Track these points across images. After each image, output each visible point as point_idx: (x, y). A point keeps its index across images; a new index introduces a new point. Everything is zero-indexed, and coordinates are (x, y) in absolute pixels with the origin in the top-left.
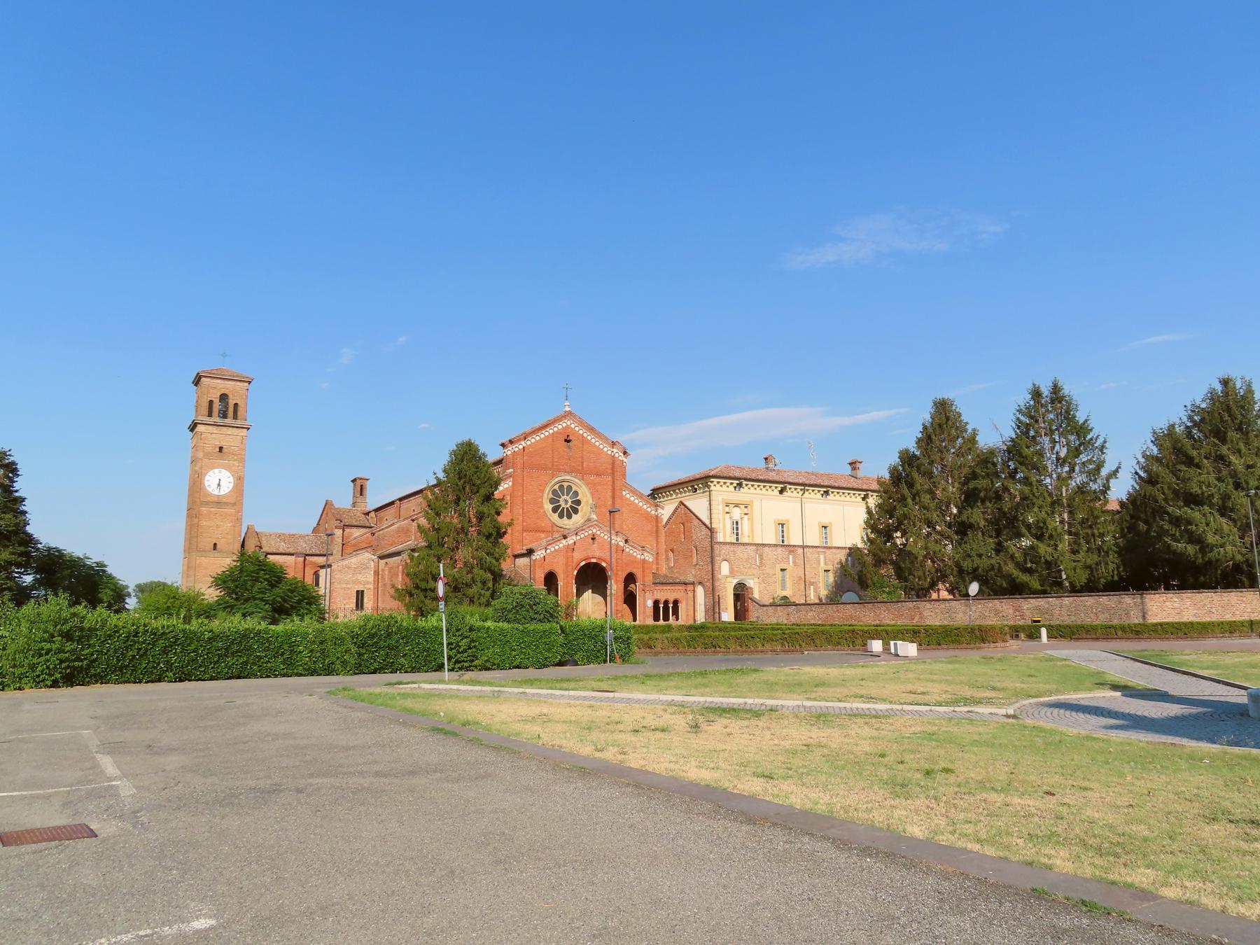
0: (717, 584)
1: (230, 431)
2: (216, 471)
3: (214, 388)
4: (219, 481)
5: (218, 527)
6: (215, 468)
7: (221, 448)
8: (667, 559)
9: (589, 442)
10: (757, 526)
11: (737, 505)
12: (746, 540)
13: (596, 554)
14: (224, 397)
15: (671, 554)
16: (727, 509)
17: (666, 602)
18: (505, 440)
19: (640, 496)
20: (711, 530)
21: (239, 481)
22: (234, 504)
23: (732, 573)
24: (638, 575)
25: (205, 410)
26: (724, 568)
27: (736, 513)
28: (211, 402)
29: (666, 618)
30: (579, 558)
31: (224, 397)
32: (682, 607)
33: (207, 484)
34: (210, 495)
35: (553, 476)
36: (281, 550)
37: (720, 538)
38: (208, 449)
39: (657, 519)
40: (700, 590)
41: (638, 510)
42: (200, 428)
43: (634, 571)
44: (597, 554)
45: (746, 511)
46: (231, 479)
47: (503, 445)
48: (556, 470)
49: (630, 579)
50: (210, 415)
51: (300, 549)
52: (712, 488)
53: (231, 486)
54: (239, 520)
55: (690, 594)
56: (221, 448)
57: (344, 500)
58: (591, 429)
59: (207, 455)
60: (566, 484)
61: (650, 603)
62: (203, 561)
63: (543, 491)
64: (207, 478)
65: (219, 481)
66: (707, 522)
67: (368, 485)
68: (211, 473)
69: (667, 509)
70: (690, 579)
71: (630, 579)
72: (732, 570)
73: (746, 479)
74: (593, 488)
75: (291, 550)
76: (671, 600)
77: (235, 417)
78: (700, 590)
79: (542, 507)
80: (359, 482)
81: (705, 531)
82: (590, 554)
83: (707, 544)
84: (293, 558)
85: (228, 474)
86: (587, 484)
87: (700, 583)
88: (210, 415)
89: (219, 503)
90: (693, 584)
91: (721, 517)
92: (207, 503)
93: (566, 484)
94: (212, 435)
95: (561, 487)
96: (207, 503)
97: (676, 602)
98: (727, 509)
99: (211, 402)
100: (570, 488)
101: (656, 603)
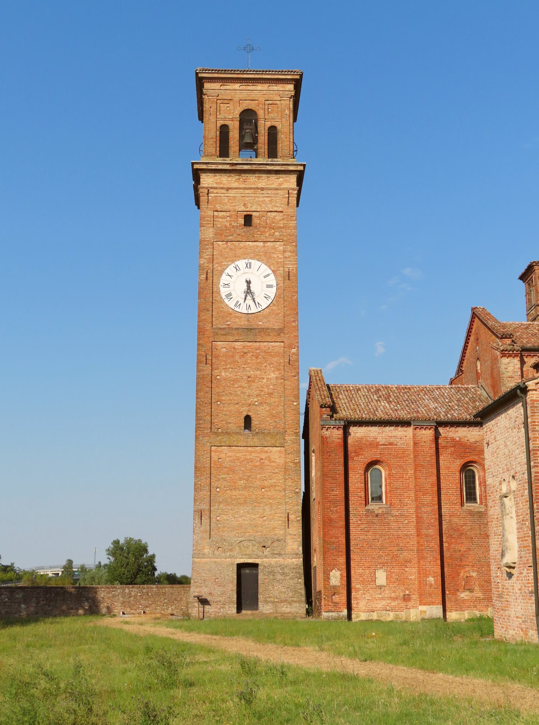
1: (263, 181)
2: (242, 263)
3: (228, 102)
4: (248, 283)
5: (250, 380)
7: (248, 220)
14: (248, 118)
21: (288, 281)
22: (280, 331)
25: (213, 147)
28: (224, 130)
31: (248, 118)
33: (224, 292)
34: (231, 313)
36: (380, 415)
38: (223, 221)
42: (206, 180)
46: (272, 280)
50: (224, 152)
53: (272, 292)
54: (292, 364)
56: (248, 220)
59: (221, 235)
64: (224, 279)
65: (248, 283)
68: (230, 270)
75: (403, 415)
77: (273, 153)
84: (409, 431)
85: (265, 269)
88: (224, 152)
89: (251, 330)
92: (228, 331)
94: (229, 194)
99: (224, 130)
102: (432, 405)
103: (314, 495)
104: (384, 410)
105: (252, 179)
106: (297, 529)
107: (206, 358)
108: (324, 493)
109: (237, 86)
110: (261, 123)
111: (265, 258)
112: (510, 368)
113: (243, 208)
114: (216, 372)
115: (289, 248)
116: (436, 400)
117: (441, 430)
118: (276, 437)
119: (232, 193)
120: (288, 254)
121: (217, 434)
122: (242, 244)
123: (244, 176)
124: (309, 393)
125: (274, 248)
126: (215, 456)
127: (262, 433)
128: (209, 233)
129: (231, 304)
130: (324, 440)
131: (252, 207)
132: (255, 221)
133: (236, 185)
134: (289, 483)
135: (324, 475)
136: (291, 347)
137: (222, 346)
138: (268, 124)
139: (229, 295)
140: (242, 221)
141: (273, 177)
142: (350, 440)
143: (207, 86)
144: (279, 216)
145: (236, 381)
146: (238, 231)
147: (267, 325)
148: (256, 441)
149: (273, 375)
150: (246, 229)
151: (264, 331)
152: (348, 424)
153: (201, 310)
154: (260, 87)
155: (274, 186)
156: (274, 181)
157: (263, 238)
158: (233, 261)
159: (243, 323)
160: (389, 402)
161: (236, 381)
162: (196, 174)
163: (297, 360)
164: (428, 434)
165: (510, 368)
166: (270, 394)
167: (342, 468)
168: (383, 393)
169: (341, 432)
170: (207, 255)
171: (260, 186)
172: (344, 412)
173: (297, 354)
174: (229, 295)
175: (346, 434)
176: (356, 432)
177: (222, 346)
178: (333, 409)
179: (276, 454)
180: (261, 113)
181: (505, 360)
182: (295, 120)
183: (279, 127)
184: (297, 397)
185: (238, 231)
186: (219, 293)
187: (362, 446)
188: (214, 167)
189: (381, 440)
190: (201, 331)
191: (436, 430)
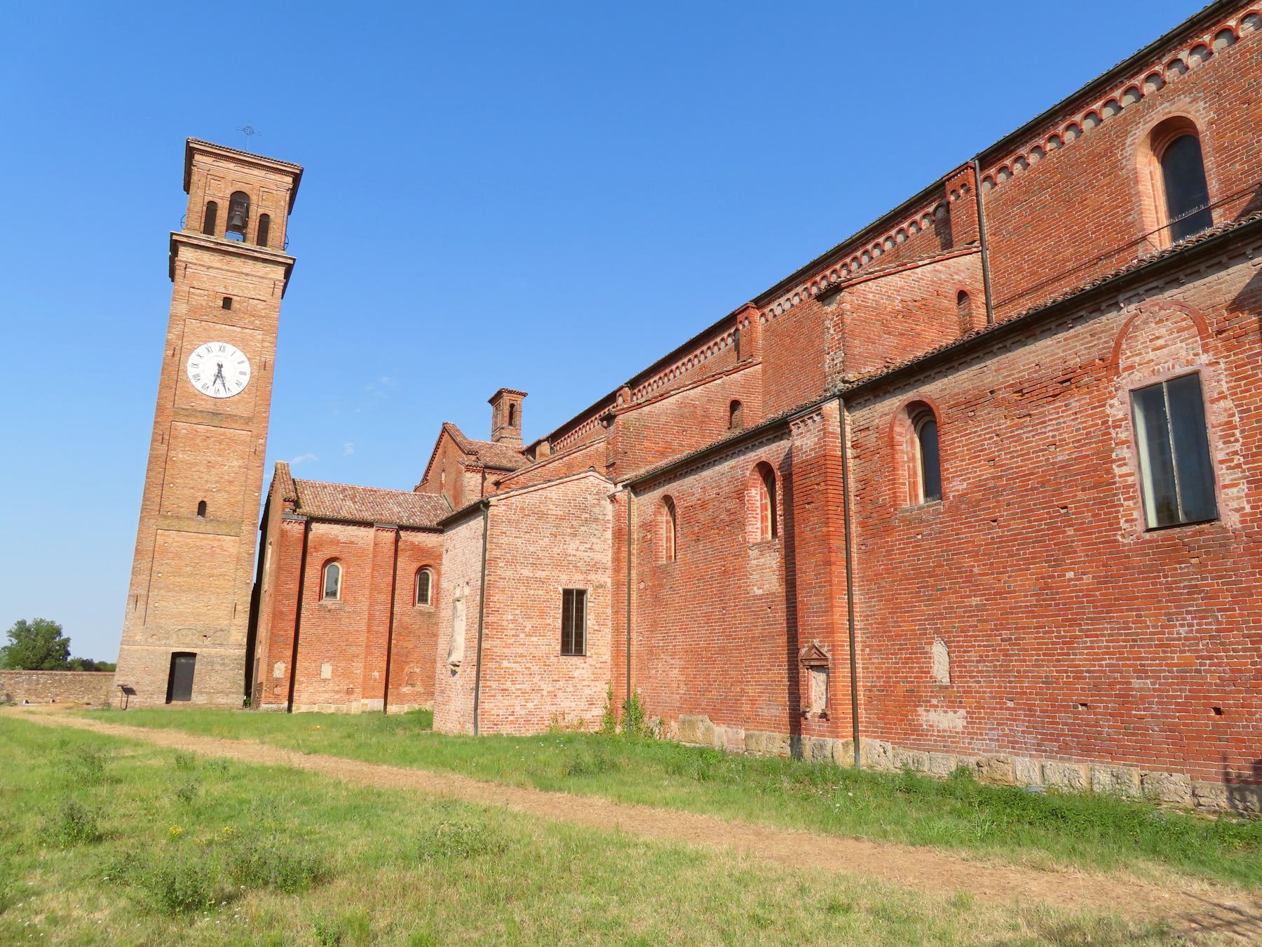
2: (215, 346)
3: (219, 180)
4: (219, 367)
6: (211, 339)
7: (227, 303)
14: (239, 200)
22: (248, 420)
25: (198, 222)
28: (212, 208)
31: (239, 200)
33: (191, 371)
34: (198, 395)
36: (344, 514)
38: (199, 299)
42: (185, 254)
46: (246, 367)
50: (209, 228)
51: (386, 515)
53: (245, 380)
56: (227, 303)
57: (477, 427)
59: (194, 312)
62: (173, 539)
64: (193, 358)
65: (219, 367)
67: (524, 405)
68: (201, 350)
75: (367, 516)
77: (262, 240)
80: (506, 400)
85: (240, 355)
88: (209, 228)
89: (217, 414)
92: (191, 413)
94: (208, 272)
99: (212, 208)
102: (396, 509)
103: (266, 586)
104: (348, 509)
105: (237, 262)
106: (243, 620)
107: (162, 437)
108: (277, 587)
109: (231, 165)
110: (253, 208)
111: (242, 344)
112: (472, 483)
114: (172, 453)
115: (268, 338)
116: (400, 505)
117: (402, 533)
118: (231, 526)
119: (212, 273)
120: (266, 344)
121: (166, 517)
122: (218, 326)
123: (228, 258)
124: (272, 486)
125: (252, 335)
127: (215, 520)
128: (182, 309)
129: (198, 385)
130: (283, 534)
131: (232, 291)
132: (235, 305)
133: (218, 265)
134: (240, 573)
135: (279, 568)
136: (258, 437)
137: (182, 427)
138: (261, 211)
139: (197, 377)
140: (221, 303)
141: (260, 265)
142: (311, 536)
143: (197, 157)
144: (261, 305)
145: (195, 464)
146: (215, 312)
147: (234, 412)
148: (209, 528)
149: (235, 463)
150: (224, 311)
151: (230, 417)
152: (310, 520)
153: (163, 386)
154: (256, 172)
155: (260, 274)
156: (260, 269)
157: (241, 324)
158: (205, 342)
159: (209, 406)
160: (355, 503)
161: (195, 464)
162: (175, 246)
163: (264, 451)
164: (389, 536)
165: (472, 483)
166: (230, 482)
167: (299, 563)
168: (349, 493)
169: (302, 527)
170: (177, 330)
171: (245, 271)
172: (308, 508)
173: (264, 445)
174: (197, 377)
175: (307, 529)
177: (182, 427)
178: (297, 504)
179: (230, 544)
180: (254, 198)
181: (468, 475)
182: (289, 212)
183: (272, 217)
184: (259, 488)
185: (215, 312)
186: (185, 372)
187: (321, 543)
188: (195, 242)
189: (342, 538)
190: (160, 409)
191: (397, 533)
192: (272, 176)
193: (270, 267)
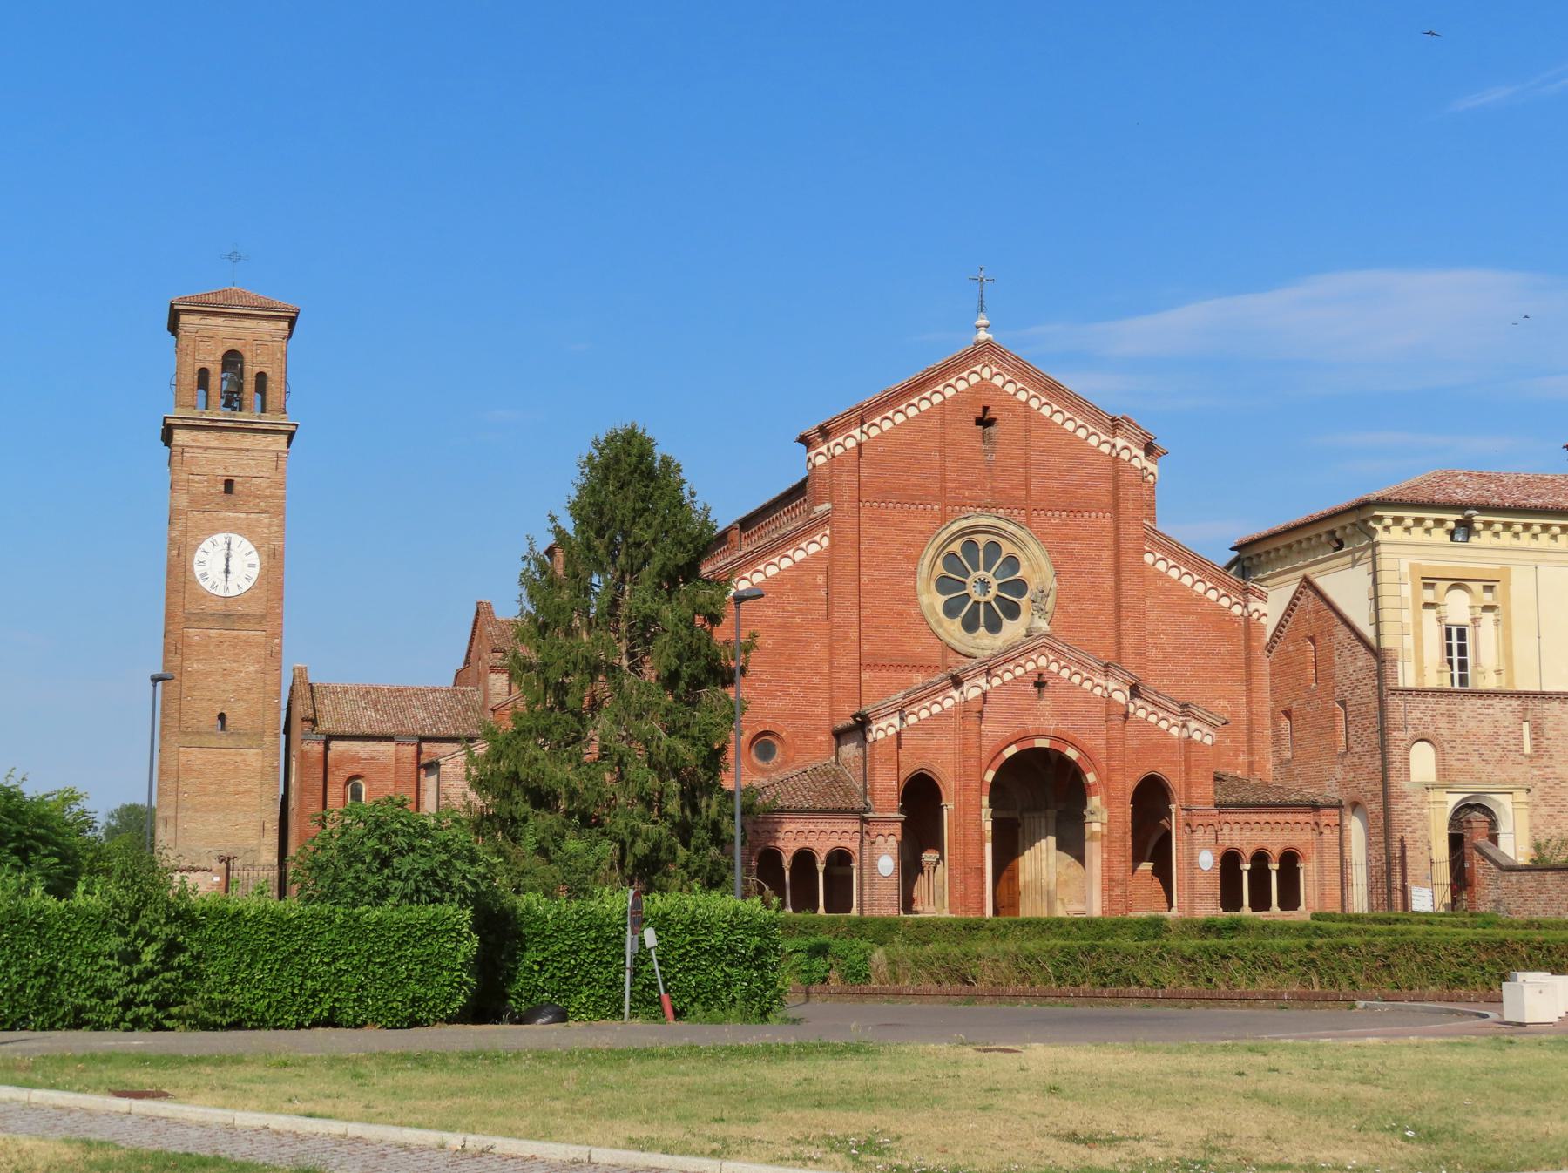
0: (1397, 807)
1: (248, 441)
3: (212, 337)
4: (226, 564)
5: (226, 673)
6: (215, 531)
7: (229, 485)
8: (1277, 739)
9: (1046, 423)
10: (1523, 646)
11: (1458, 584)
12: (1490, 682)
13: (1045, 724)
14: (232, 360)
15: (1285, 723)
16: (1429, 596)
17: (1260, 858)
18: (810, 427)
19: (1198, 564)
20: (1377, 653)
21: (273, 560)
22: (263, 618)
23: (1446, 778)
24: (1175, 781)
26: (1422, 763)
27: (1458, 607)
29: (1261, 902)
30: (1001, 736)
31: (232, 360)
32: (1308, 874)
33: (198, 570)
35: (944, 519)
36: (364, 729)
37: (1406, 676)
38: (200, 487)
39: (1249, 626)
40: (1355, 828)
41: (1190, 604)
42: (180, 437)
43: (1163, 771)
44: (1051, 726)
45: (1488, 598)
46: (255, 558)
47: (804, 440)
48: (949, 502)
49: (1151, 798)
51: (409, 725)
52: (1381, 536)
53: (255, 573)
54: (275, 656)
55: (1330, 837)
56: (229, 485)
58: (1052, 389)
59: (196, 502)
60: (982, 540)
61: (1207, 860)
62: (195, 756)
63: (915, 560)
65: (226, 564)
66: (1369, 633)
69: (1271, 604)
70: (1332, 793)
71: (1151, 798)
72: (1443, 767)
73: (1484, 509)
74: (1057, 545)
75: (388, 728)
76: (1275, 850)
78: (1355, 828)
79: (915, 602)
81: (1364, 659)
82: (1031, 727)
83: (1369, 692)
84: (391, 746)
86: (1041, 539)
87: (1355, 806)
89: (228, 615)
90: (1338, 806)
91: (1407, 617)
92: (200, 618)
93: (982, 540)
94: (210, 455)
95: (970, 547)
96: (200, 618)
97: (1290, 859)
98: (1429, 596)
99: (203, 374)
100: (994, 548)
101: (1230, 860)
102: (422, 715)
103: (293, 803)
104: (370, 720)
105: (236, 436)
106: (272, 839)
107: (174, 645)
108: (302, 806)
109: (220, 321)
110: (247, 367)
111: (248, 531)
112: (498, 684)
113: (222, 472)
114: (186, 664)
115: (276, 521)
116: (426, 707)
117: (424, 746)
118: (254, 738)
120: (274, 529)
121: (186, 734)
122: (221, 515)
123: (226, 434)
124: (292, 690)
125: (258, 520)
126: (183, 758)
127: (236, 733)
128: (183, 500)
129: (206, 585)
130: (304, 754)
131: (233, 472)
132: (237, 488)
133: (215, 444)
134: (266, 788)
135: (302, 790)
136: (274, 636)
137: (194, 634)
138: (257, 369)
139: (204, 575)
141: (260, 436)
142: (330, 754)
143: (184, 318)
144: (265, 483)
145: (209, 674)
146: (217, 500)
147: (247, 611)
148: (230, 742)
149: (252, 668)
150: (226, 497)
151: (243, 617)
152: (331, 737)
153: (170, 591)
154: (247, 323)
156: (261, 441)
157: (245, 508)
158: (210, 535)
159: (220, 608)
160: (377, 711)
161: (209, 674)
162: (167, 437)
163: (280, 653)
164: (410, 750)
165: (498, 684)
166: (248, 690)
167: (321, 783)
168: (371, 696)
169: (321, 746)
170: (179, 526)
171: (244, 445)
172: (327, 725)
173: (280, 645)
174: (204, 575)
175: (327, 748)
176: (337, 747)
177: (194, 634)
178: (314, 722)
179: (253, 758)
180: (247, 356)
181: (493, 676)
182: (289, 337)
183: (269, 374)
184: (279, 694)
185: (217, 500)
186: (192, 572)
187: (343, 760)
188: (190, 422)
189: (363, 754)
190: (169, 616)
191: (419, 747)
192: (266, 324)
193: (270, 438)
